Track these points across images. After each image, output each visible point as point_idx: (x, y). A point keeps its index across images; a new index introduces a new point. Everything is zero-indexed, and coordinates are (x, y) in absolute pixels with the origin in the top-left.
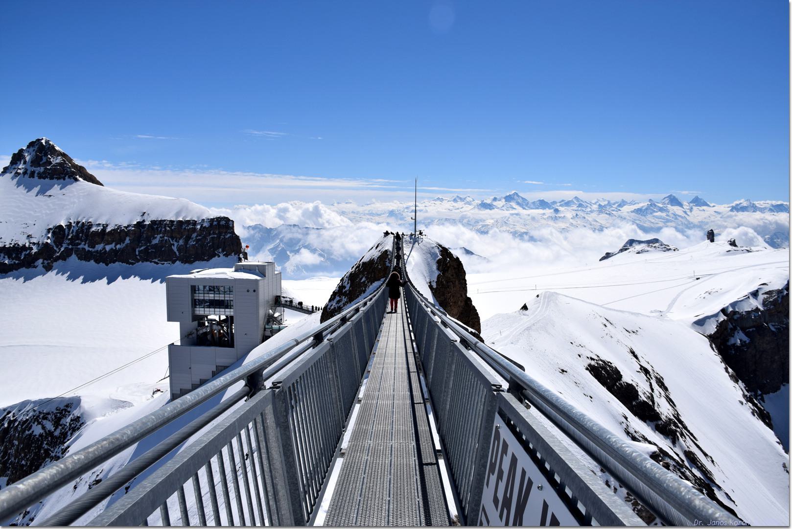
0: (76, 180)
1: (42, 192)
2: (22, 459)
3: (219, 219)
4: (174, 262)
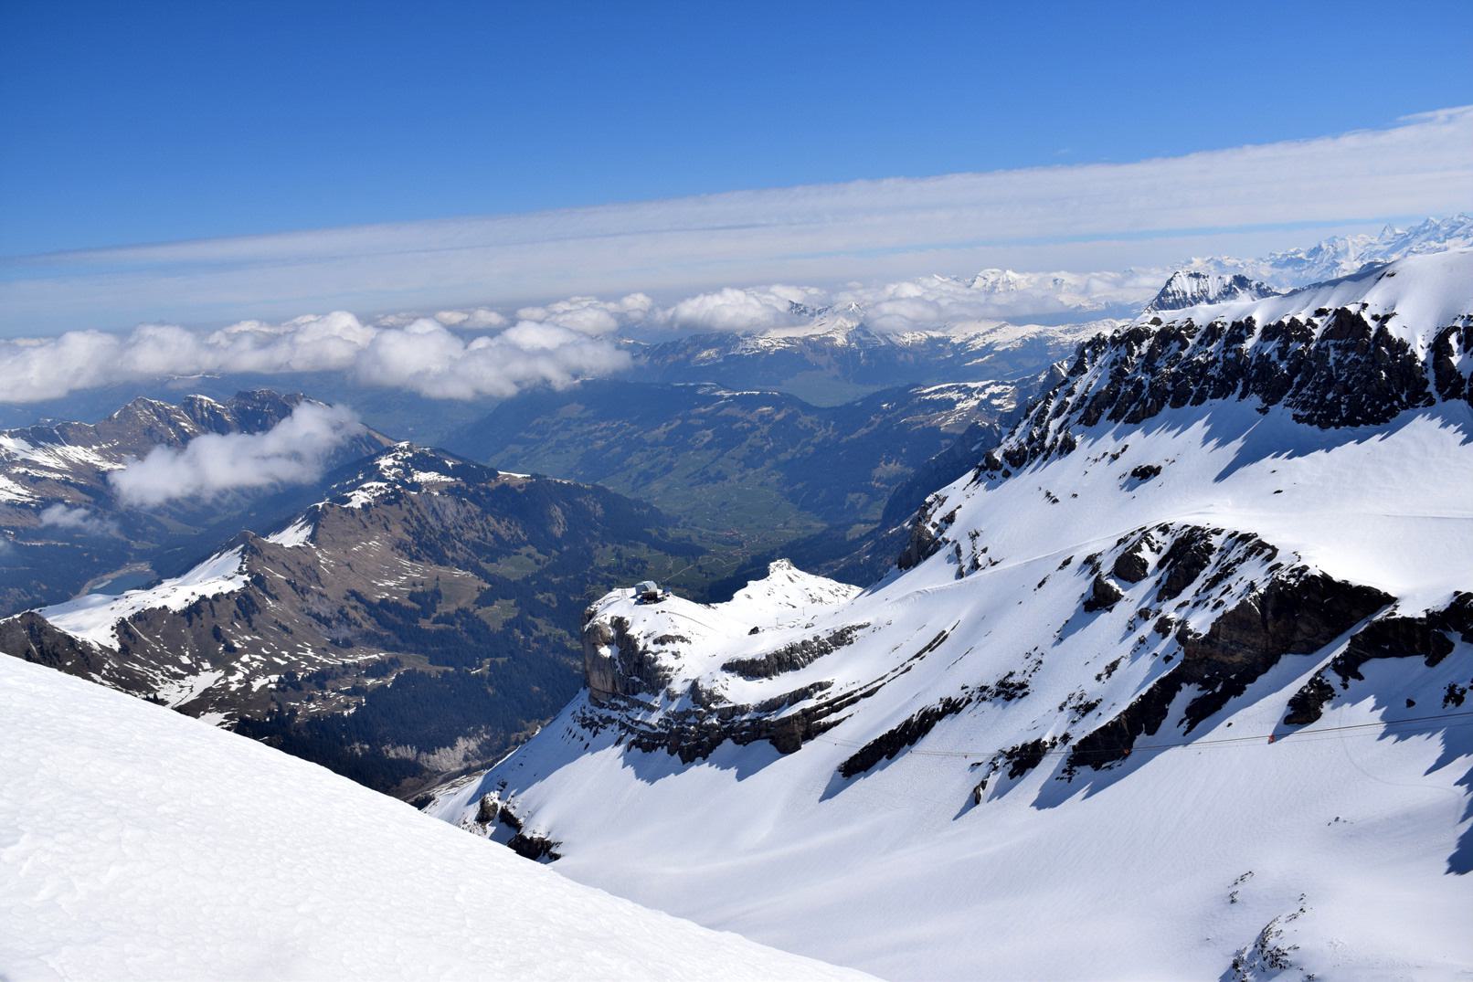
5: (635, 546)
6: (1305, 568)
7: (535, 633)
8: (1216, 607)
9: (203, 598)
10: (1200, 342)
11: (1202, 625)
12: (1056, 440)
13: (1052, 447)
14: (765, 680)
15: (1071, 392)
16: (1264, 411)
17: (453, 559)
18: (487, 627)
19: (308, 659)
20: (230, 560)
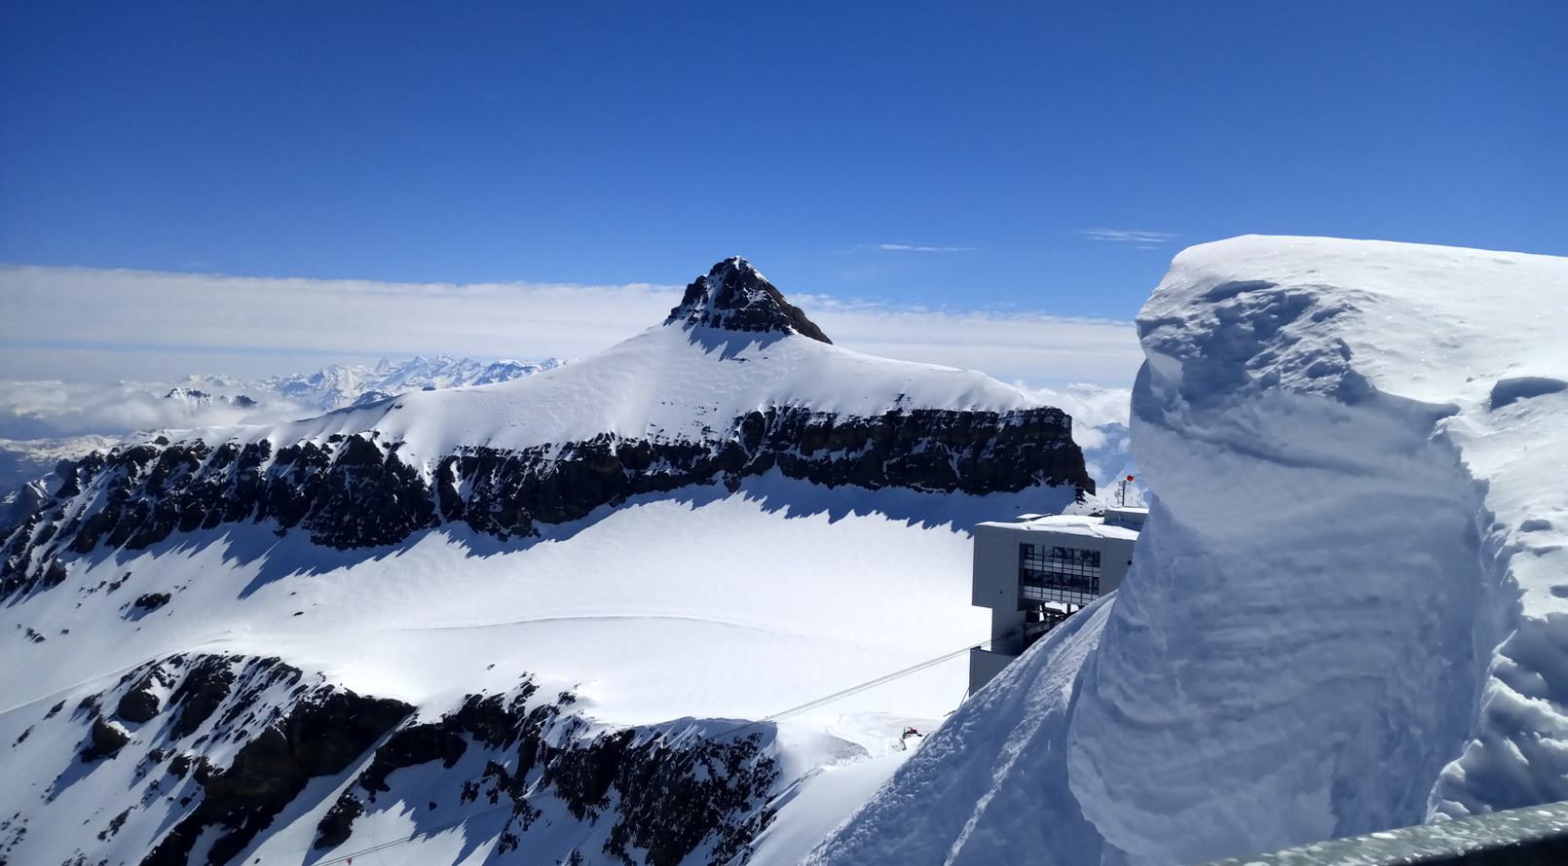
0: (787, 333)
1: (730, 354)
2: (674, 821)
3: (1043, 413)
4: (950, 490)
6: (331, 687)
8: (237, 739)
10: (212, 464)
11: (223, 759)
12: (40, 569)
13: (35, 578)
15: (59, 516)
16: (282, 534)
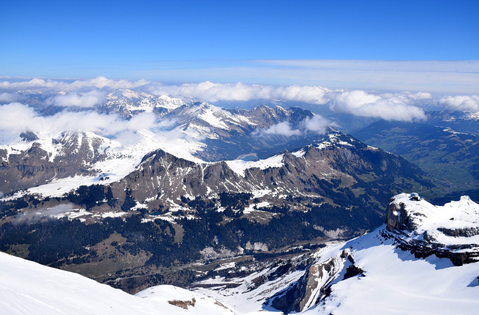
5: (410, 179)
7: (369, 201)
9: (270, 167)
14: (453, 237)
17: (347, 171)
18: (354, 195)
19: (296, 192)
20: (280, 158)
